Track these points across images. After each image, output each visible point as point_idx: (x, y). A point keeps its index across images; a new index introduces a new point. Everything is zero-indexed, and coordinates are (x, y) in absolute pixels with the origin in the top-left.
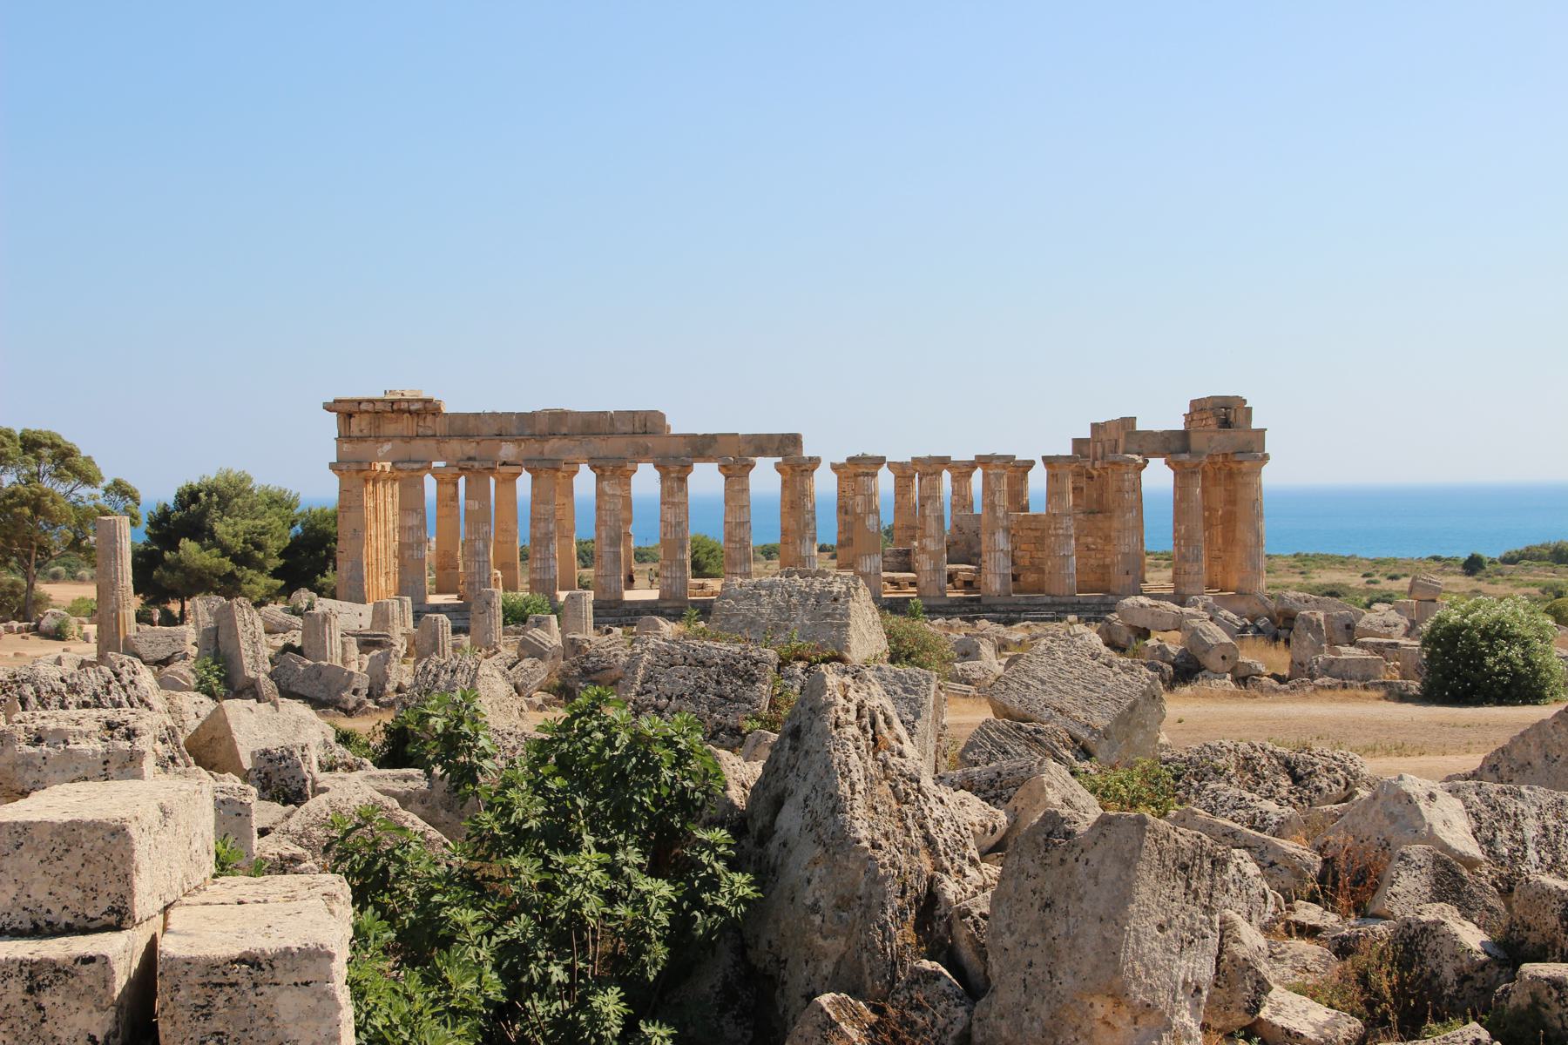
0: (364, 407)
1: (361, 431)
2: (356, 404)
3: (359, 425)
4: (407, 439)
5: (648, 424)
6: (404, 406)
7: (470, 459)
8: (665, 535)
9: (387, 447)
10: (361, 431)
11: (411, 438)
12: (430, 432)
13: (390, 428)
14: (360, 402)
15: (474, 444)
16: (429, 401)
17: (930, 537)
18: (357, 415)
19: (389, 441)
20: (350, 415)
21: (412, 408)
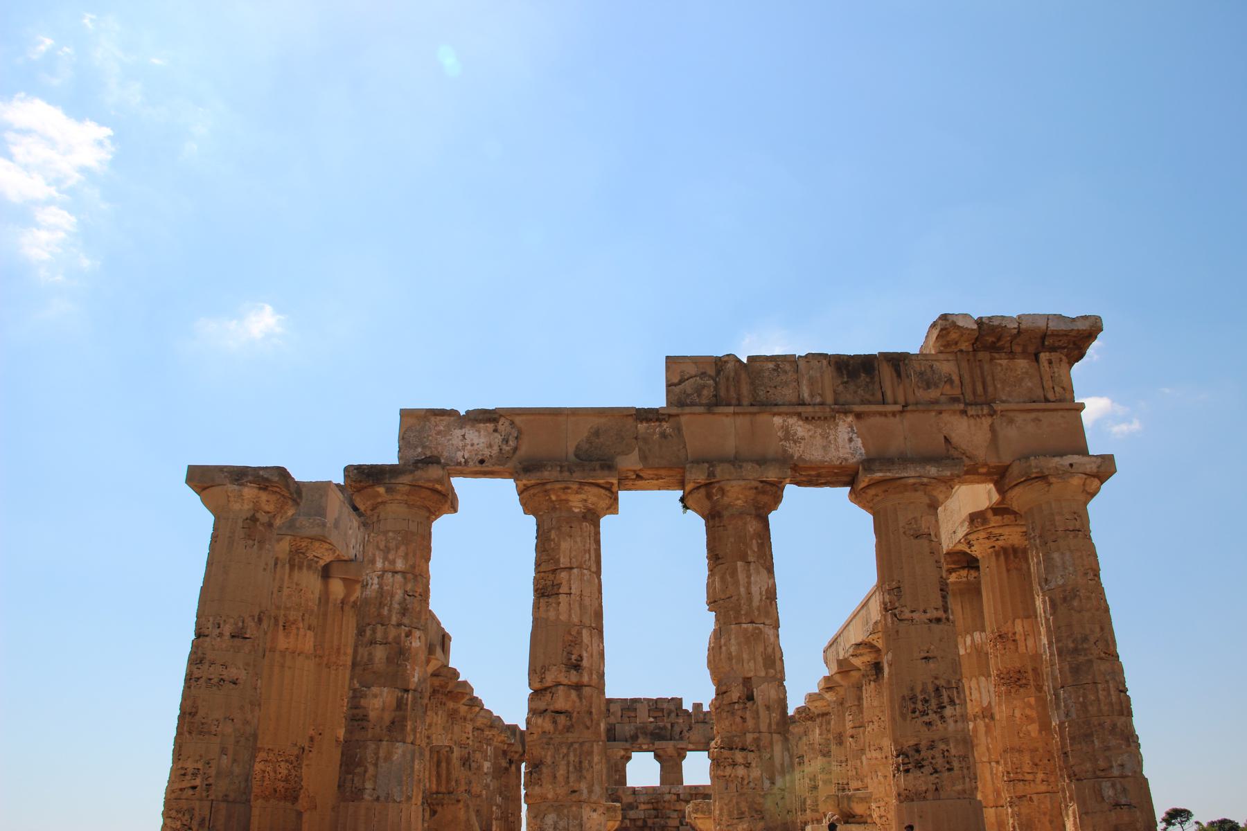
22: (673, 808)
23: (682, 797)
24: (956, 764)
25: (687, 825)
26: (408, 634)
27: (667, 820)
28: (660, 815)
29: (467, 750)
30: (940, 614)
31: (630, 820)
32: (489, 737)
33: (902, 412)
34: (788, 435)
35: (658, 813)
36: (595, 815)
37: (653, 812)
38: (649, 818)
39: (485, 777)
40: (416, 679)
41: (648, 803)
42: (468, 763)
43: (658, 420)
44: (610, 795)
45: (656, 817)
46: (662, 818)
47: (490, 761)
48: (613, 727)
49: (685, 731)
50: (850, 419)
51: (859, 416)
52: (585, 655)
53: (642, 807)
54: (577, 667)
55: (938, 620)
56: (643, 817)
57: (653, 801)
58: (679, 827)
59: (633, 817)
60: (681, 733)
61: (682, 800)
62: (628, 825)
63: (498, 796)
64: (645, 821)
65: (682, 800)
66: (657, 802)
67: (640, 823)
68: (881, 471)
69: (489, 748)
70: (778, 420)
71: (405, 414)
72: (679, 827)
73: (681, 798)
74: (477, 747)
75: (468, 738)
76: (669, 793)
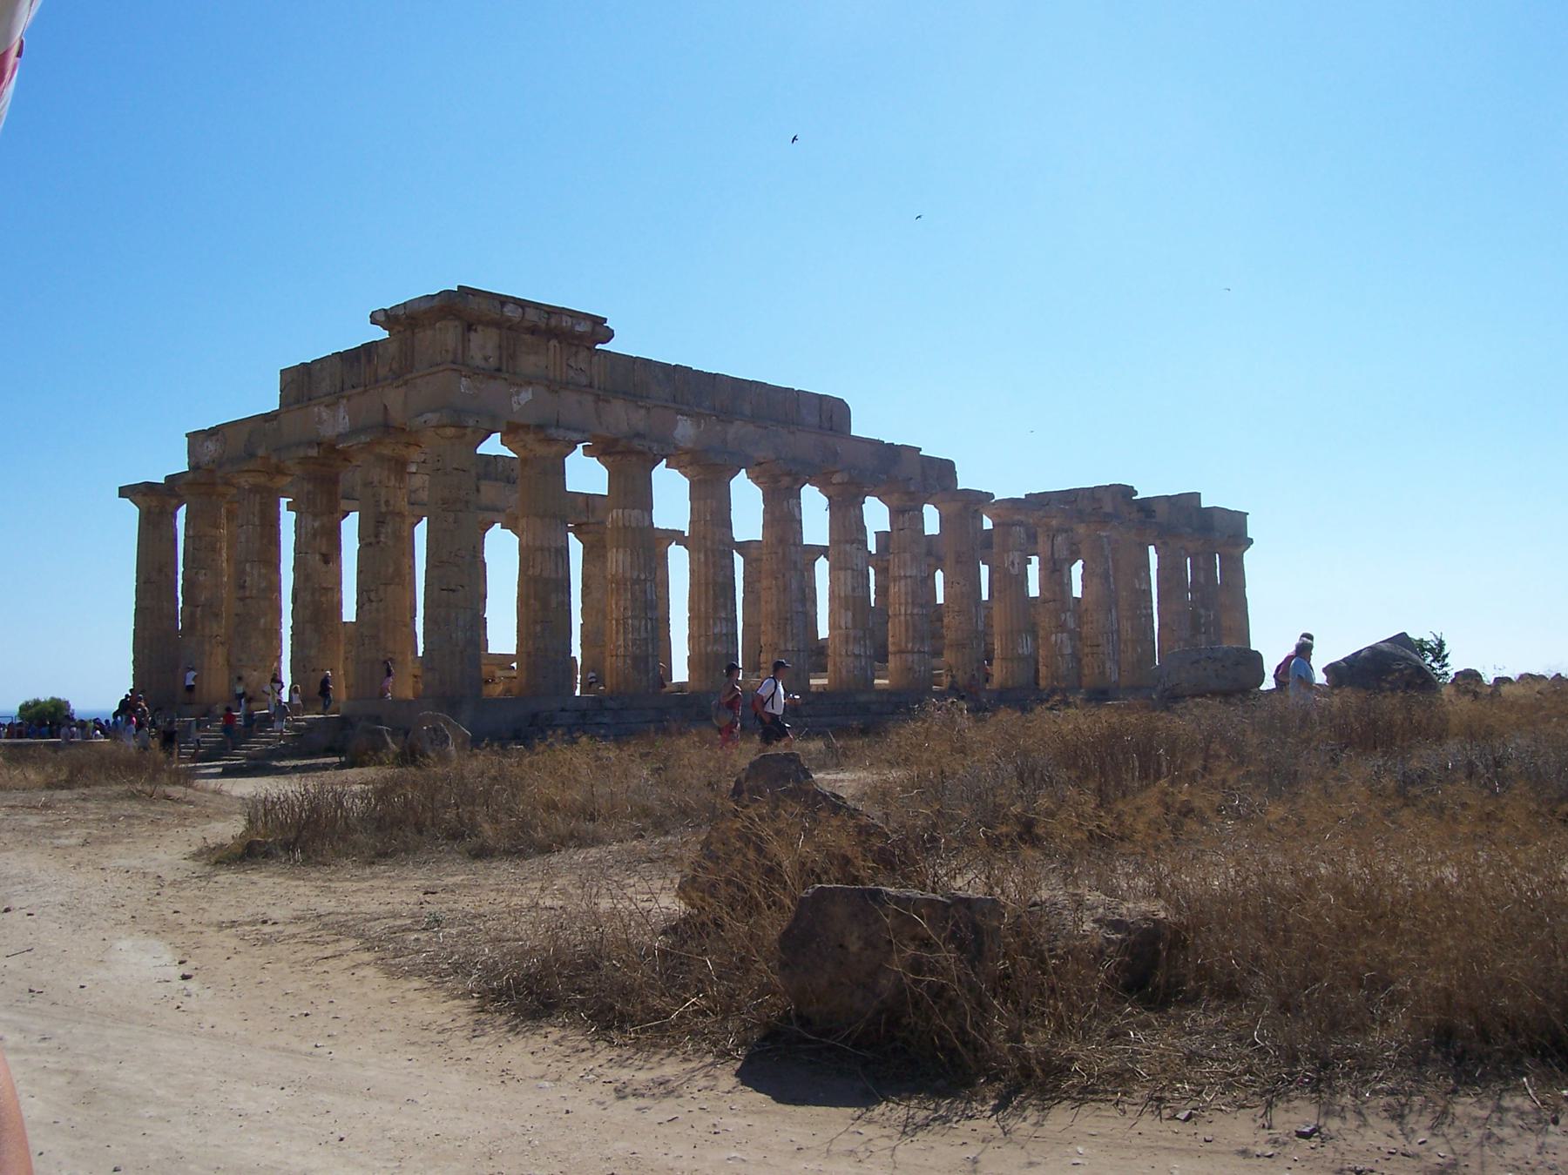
0: (509, 311)
1: (486, 359)
2: (497, 303)
3: (483, 345)
4: (554, 386)
5: (834, 418)
6: (567, 322)
7: (638, 435)
8: (854, 589)
9: (526, 395)
10: (486, 359)
11: (565, 385)
12: (584, 380)
13: (529, 363)
14: (503, 300)
15: (643, 412)
16: (599, 321)
17: (1069, 610)
18: (480, 328)
19: (530, 383)
20: (470, 327)
21: (578, 328)
24: (366, 642)
26: (197, 573)
30: (372, 540)
33: (366, 391)
34: (321, 422)
36: (255, 673)
40: (203, 599)
43: (272, 420)
50: (345, 401)
51: (349, 398)
52: (248, 579)
54: (243, 587)
55: (371, 544)
68: (342, 443)
70: (316, 409)
71: (187, 435)
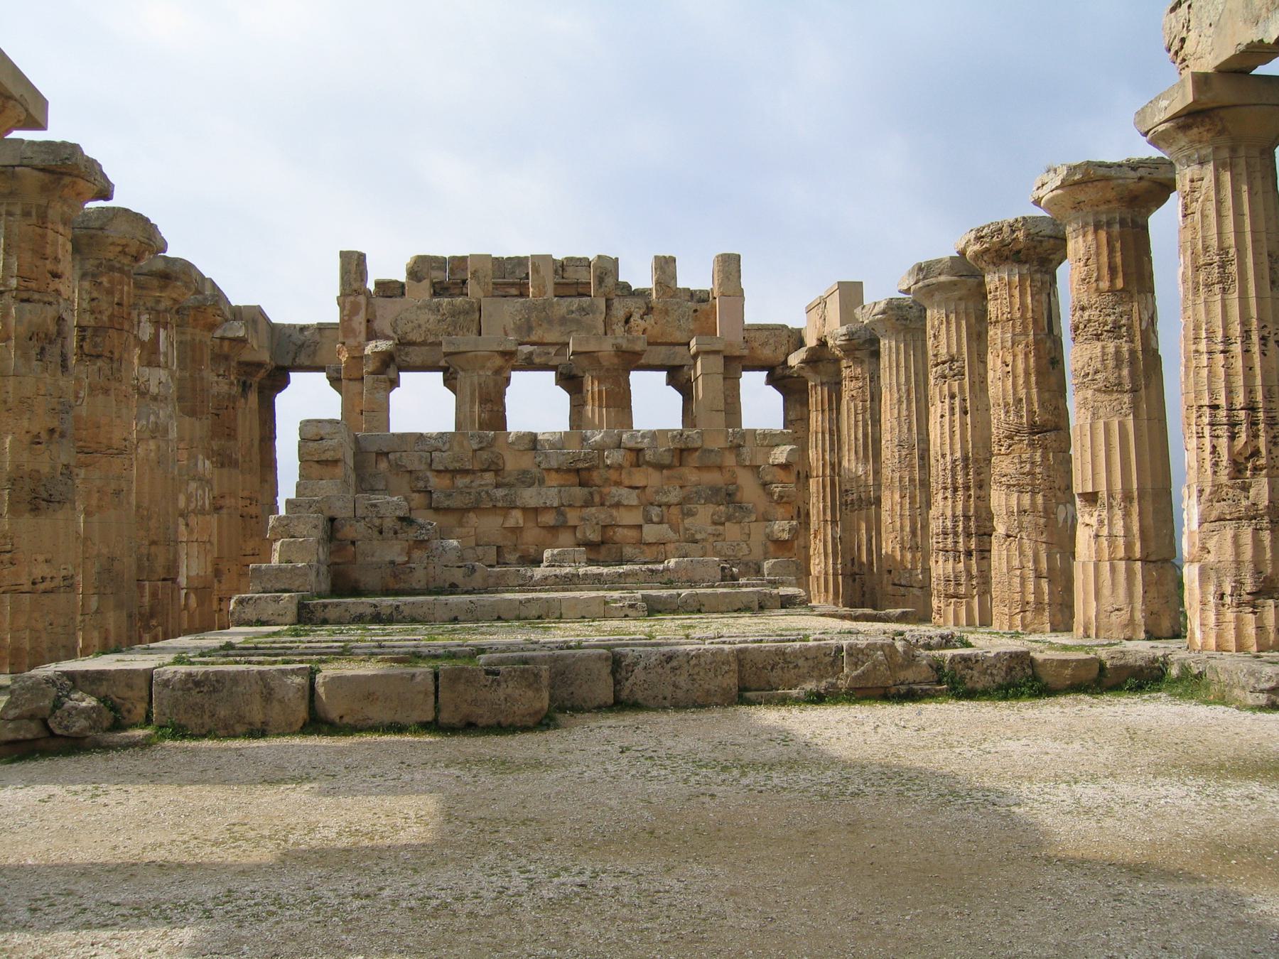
22: (627, 482)
23: (649, 456)
25: (661, 522)
27: (614, 512)
28: (597, 499)
29: (50, 312)
31: (525, 510)
32: (162, 306)
35: (591, 494)
37: (579, 492)
38: (570, 506)
39: (154, 406)
41: (569, 471)
42: (56, 350)
44: (475, 451)
45: (588, 503)
46: (602, 504)
47: (166, 367)
48: (476, 305)
49: (636, 317)
53: (553, 479)
56: (555, 505)
57: (581, 465)
58: (640, 527)
59: (533, 503)
60: (627, 321)
61: (649, 464)
62: (521, 523)
63: (201, 457)
64: (559, 510)
65: (649, 464)
66: (588, 469)
67: (549, 519)
69: (162, 333)
72: (640, 527)
73: (647, 458)
74: (111, 317)
75: (56, 275)
76: (619, 447)
